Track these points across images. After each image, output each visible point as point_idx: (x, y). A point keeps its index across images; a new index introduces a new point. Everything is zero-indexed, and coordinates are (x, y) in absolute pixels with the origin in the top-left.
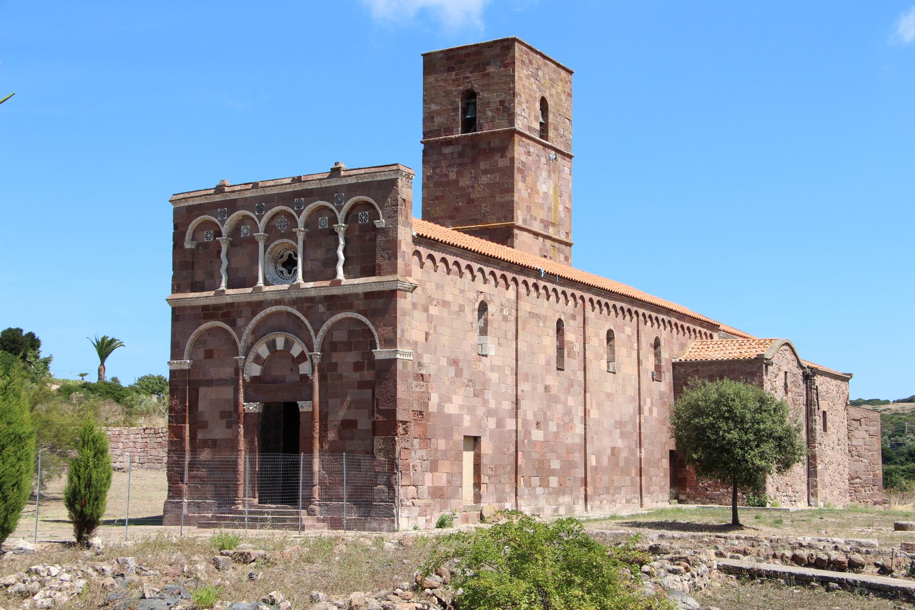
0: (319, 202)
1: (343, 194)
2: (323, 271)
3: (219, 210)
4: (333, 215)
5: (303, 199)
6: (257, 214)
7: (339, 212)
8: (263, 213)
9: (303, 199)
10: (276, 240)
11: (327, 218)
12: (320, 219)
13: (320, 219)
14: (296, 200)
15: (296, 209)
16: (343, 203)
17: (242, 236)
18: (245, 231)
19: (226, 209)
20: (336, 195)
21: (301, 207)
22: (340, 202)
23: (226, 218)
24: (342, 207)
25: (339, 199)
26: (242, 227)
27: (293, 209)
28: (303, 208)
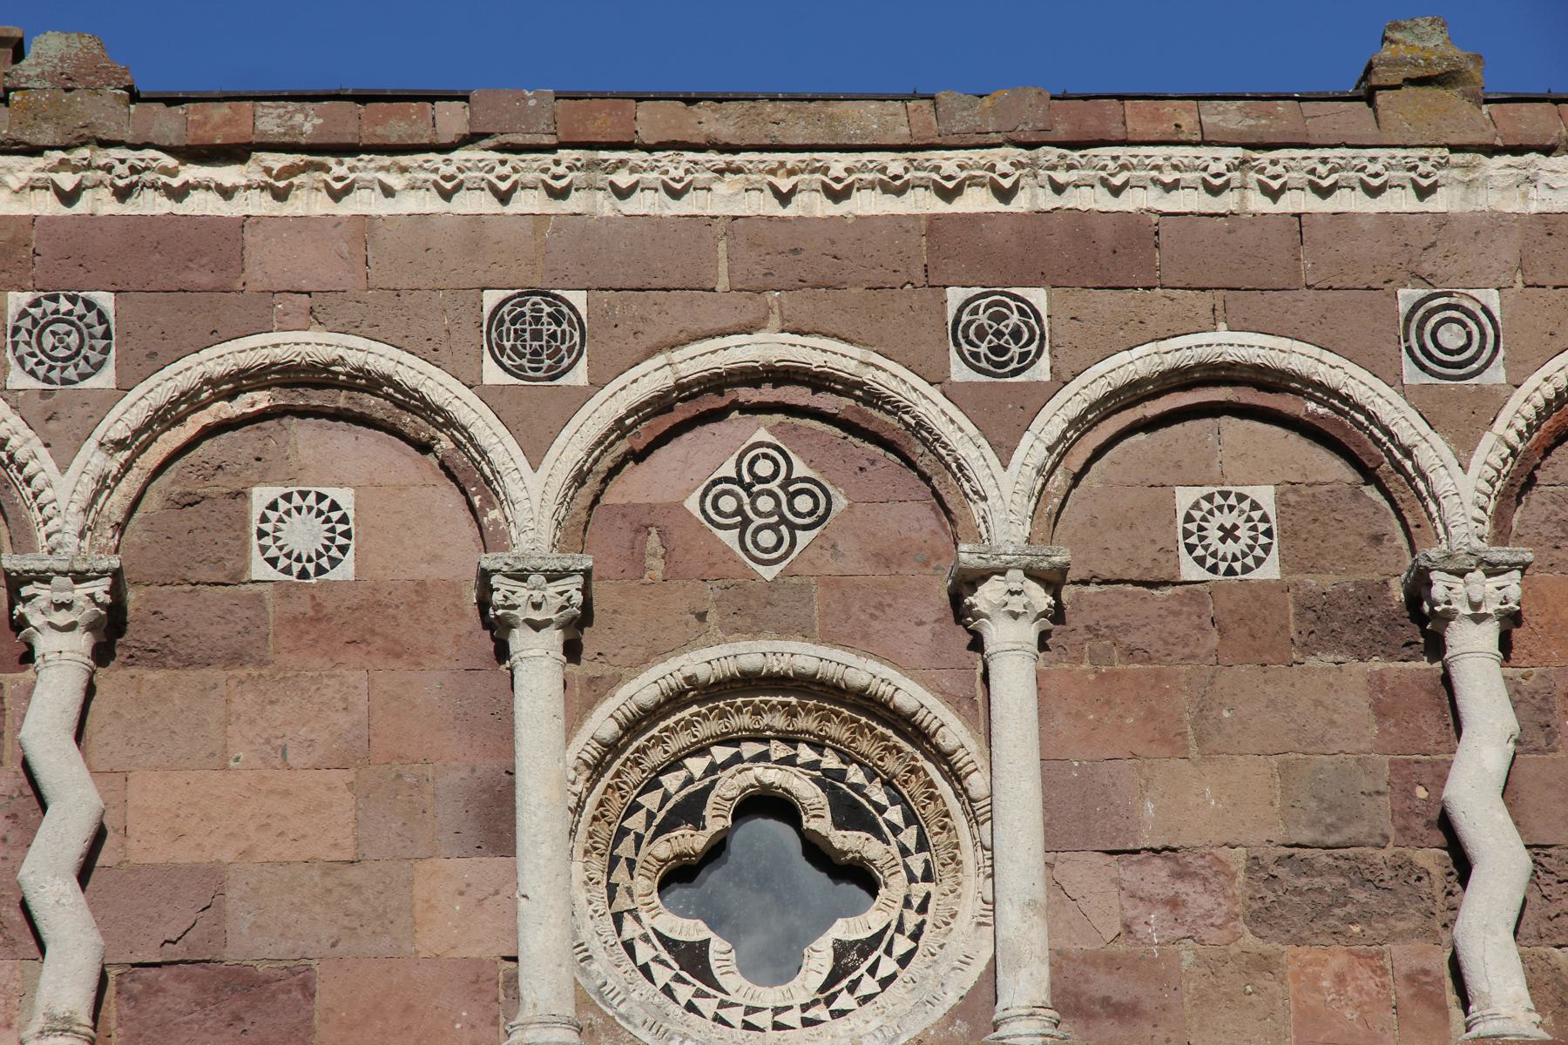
0: (1223, 335)
1: (1492, 299)
2: (1265, 964)
3: (17, 300)
4: (1335, 469)
5: (1038, 297)
6: (493, 374)
7: (1464, 446)
8: (579, 376)
9: (1038, 297)
10: (686, 645)
11: (1265, 495)
12: (1185, 497)
13: (1185, 497)
14: (955, 296)
15: (960, 372)
16: (1496, 375)
17: (259, 569)
18: (304, 534)
19: (105, 300)
20: (1407, 296)
21: (1026, 361)
22: (1458, 364)
23: (105, 379)
24: (1488, 406)
25: (1451, 337)
26: (261, 496)
27: (938, 379)
28: (1041, 370)
